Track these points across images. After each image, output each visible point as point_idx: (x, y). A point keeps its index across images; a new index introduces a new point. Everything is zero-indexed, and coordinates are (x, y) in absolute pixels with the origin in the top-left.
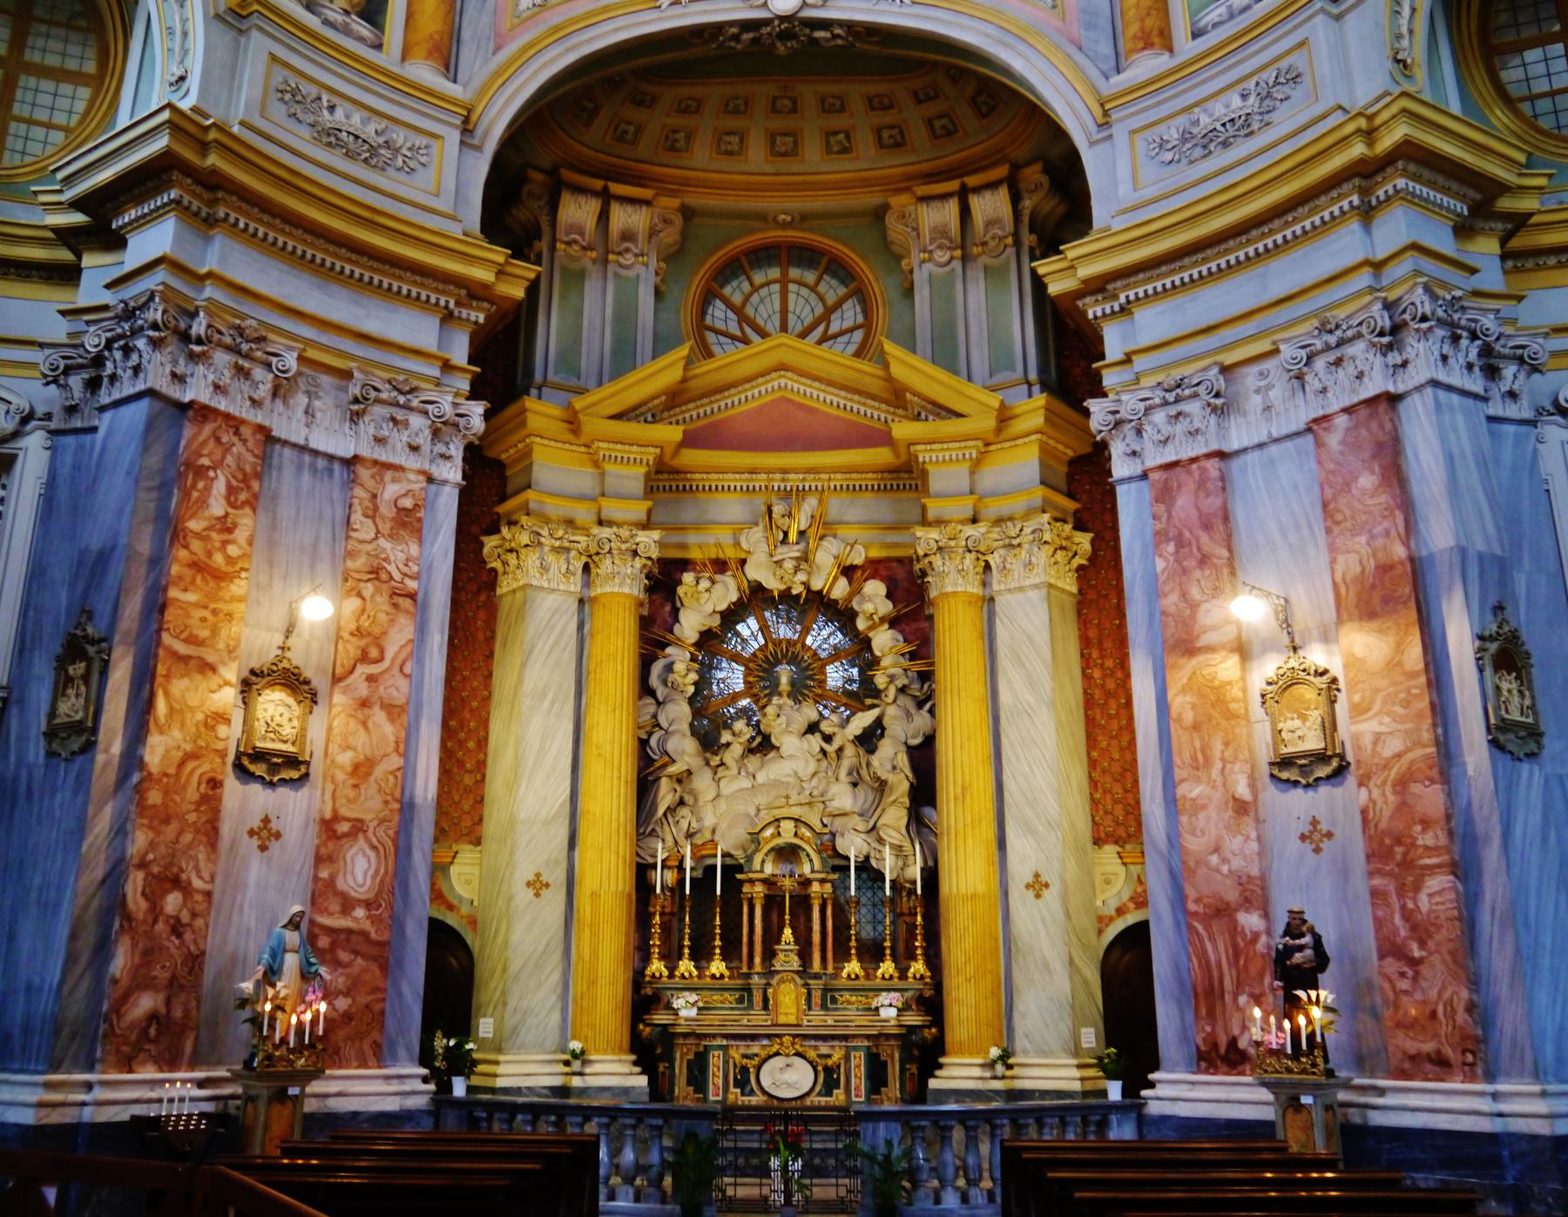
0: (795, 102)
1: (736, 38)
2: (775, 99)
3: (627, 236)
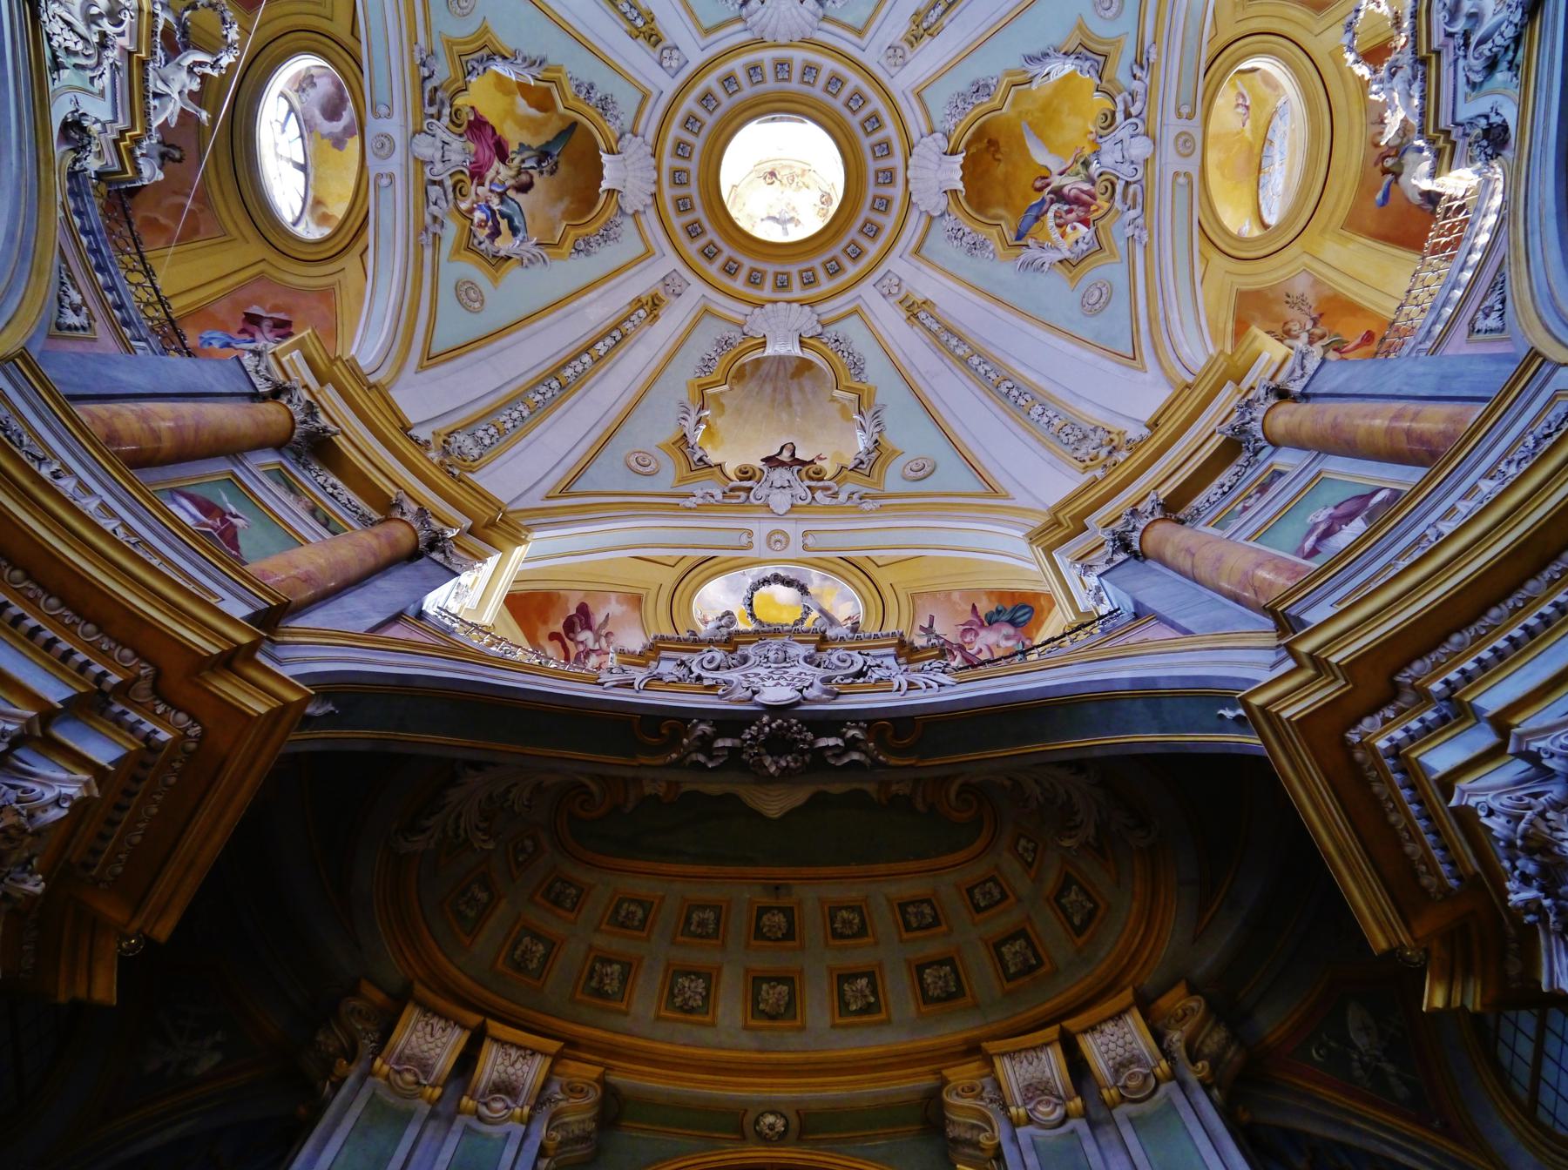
0: (791, 923)
1: (705, 743)
2: (763, 911)
3: (506, 1089)
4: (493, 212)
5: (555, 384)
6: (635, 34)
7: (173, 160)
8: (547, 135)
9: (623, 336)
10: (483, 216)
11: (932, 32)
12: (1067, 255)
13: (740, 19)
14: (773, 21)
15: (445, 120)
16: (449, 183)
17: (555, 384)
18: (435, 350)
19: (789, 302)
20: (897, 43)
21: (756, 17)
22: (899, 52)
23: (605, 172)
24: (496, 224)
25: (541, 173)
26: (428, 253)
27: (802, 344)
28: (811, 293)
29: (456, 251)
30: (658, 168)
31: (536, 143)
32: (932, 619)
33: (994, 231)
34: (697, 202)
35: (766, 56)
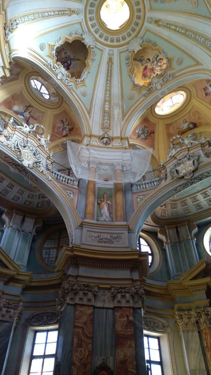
4: (157, 62)
5: (187, 33)
6: (112, 63)
7: (186, 121)
8: (137, 62)
9: (167, 24)
10: (159, 63)
11: (70, 10)
13: (96, 47)
14: (92, 40)
15: (151, 86)
16: (162, 78)
17: (187, 33)
18: (195, 63)
20: (76, 15)
21: (93, 44)
22: (78, 12)
23: (138, 50)
24: (159, 60)
25: (144, 59)
26: (177, 74)
29: (173, 69)
30: (131, 40)
31: (140, 63)
34: (131, 28)
35: (97, 36)
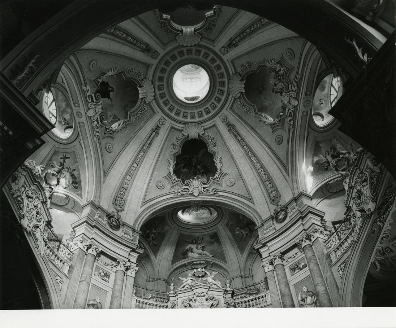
12: (172, 174)
19: (155, 92)
27: (142, 99)
28: (158, 97)
32: (69, 158)
33: (178, 150)
